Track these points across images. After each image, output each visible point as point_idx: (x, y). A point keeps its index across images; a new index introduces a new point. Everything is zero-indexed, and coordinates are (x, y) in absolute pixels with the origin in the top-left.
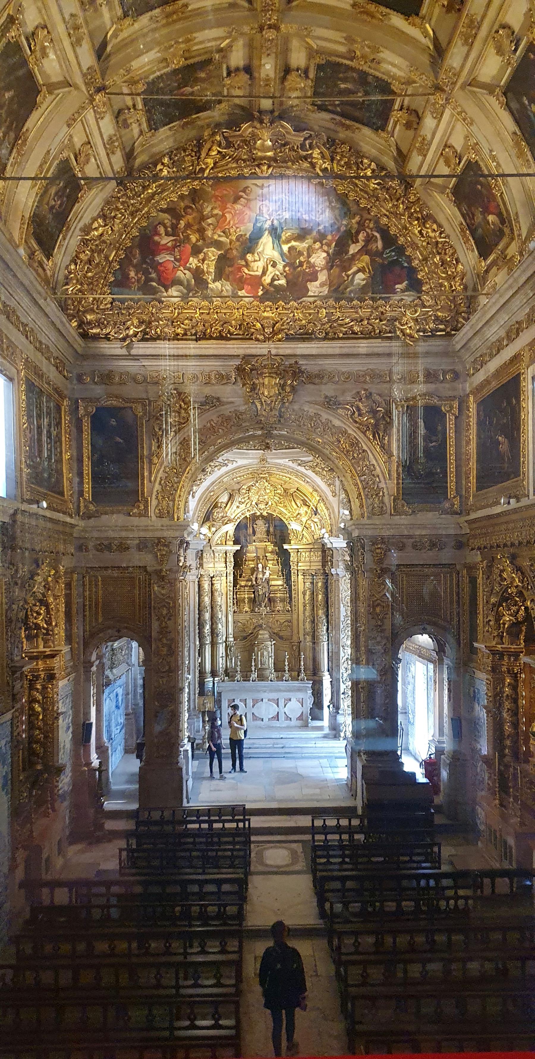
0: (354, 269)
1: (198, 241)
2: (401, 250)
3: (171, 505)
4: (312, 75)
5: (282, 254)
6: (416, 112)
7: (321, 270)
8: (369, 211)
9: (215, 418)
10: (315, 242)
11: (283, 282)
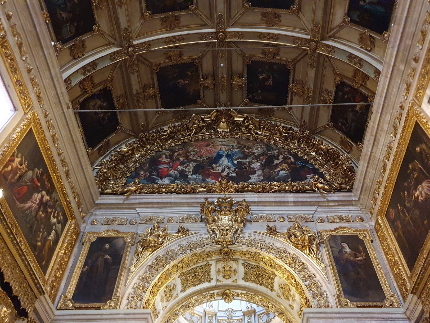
1: (184, 160)
2: (307, 162)
3: (139, 305)
4: (245, 75)
5: (233, 164)
7: (258, 170)
9: (184, 243)
10: (253, 159)
11: (234, 175)
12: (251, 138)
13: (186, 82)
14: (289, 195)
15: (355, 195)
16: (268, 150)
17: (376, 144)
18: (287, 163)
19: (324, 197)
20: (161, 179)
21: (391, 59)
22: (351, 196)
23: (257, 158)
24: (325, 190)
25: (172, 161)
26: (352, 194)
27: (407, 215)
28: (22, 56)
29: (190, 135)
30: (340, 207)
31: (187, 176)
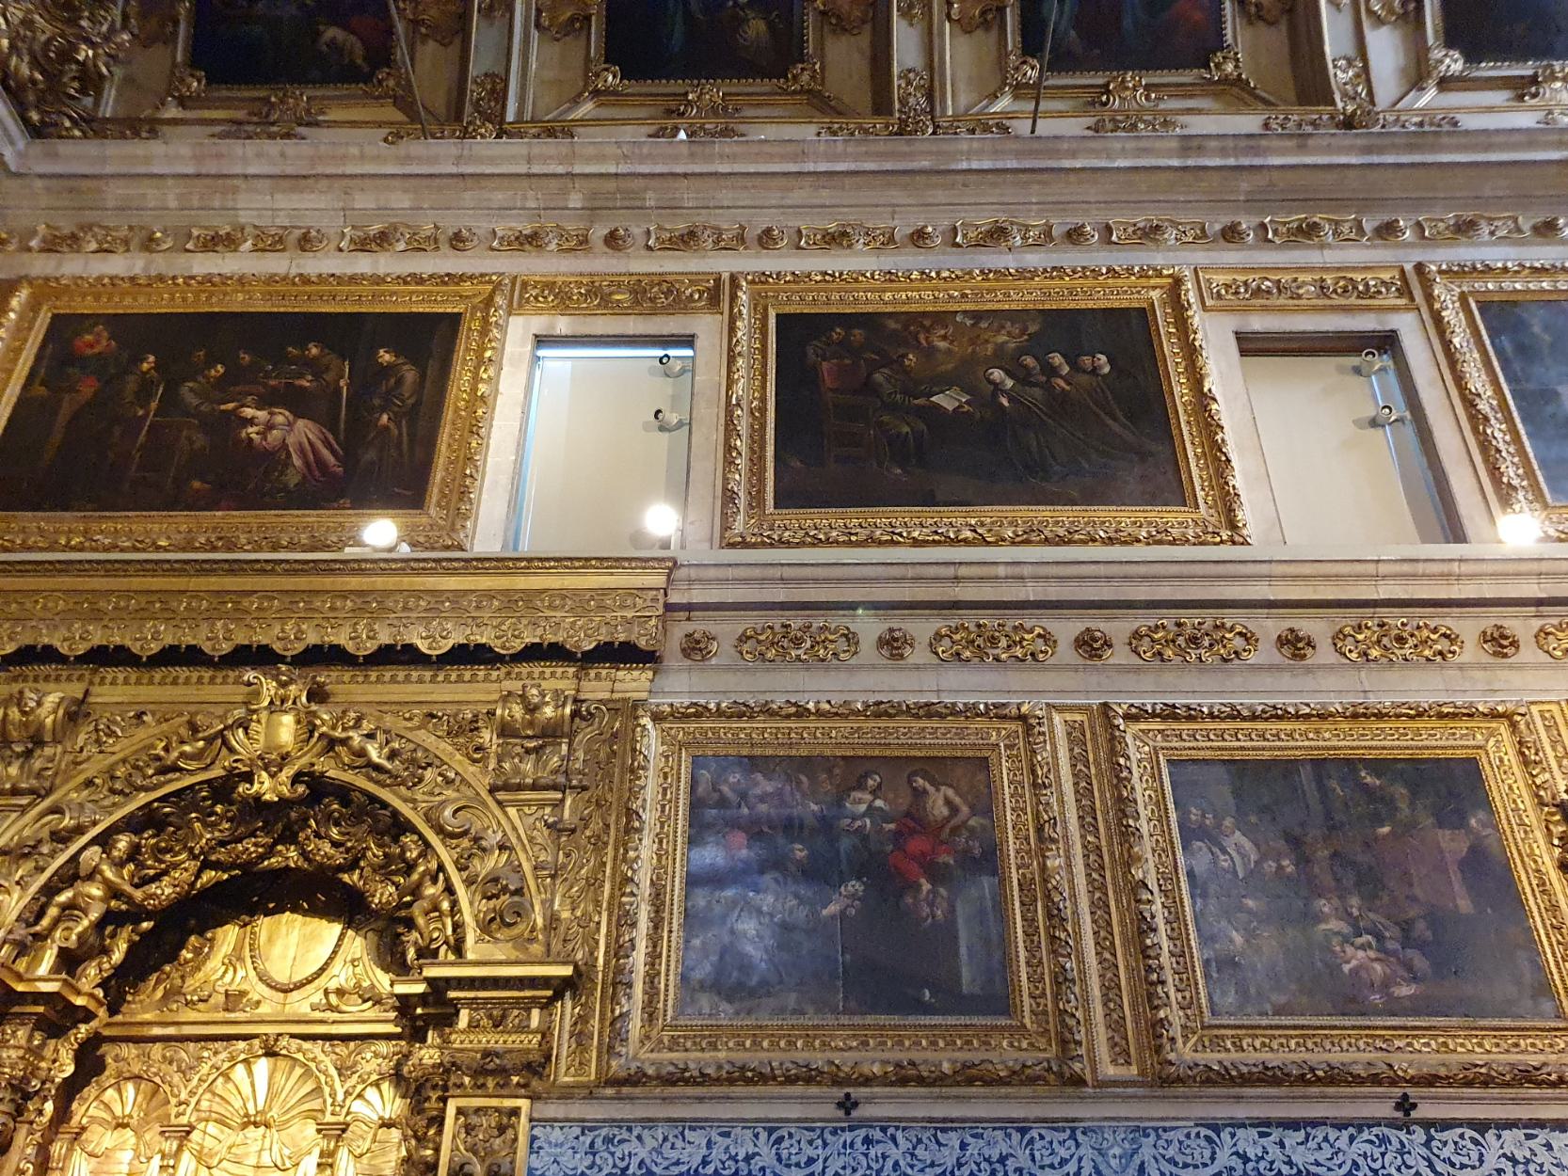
15: (20, 155)
17: (286, 184)
21: (589, 160)
22: (12, 143)
26: (21, 144)
27: (154, 405)
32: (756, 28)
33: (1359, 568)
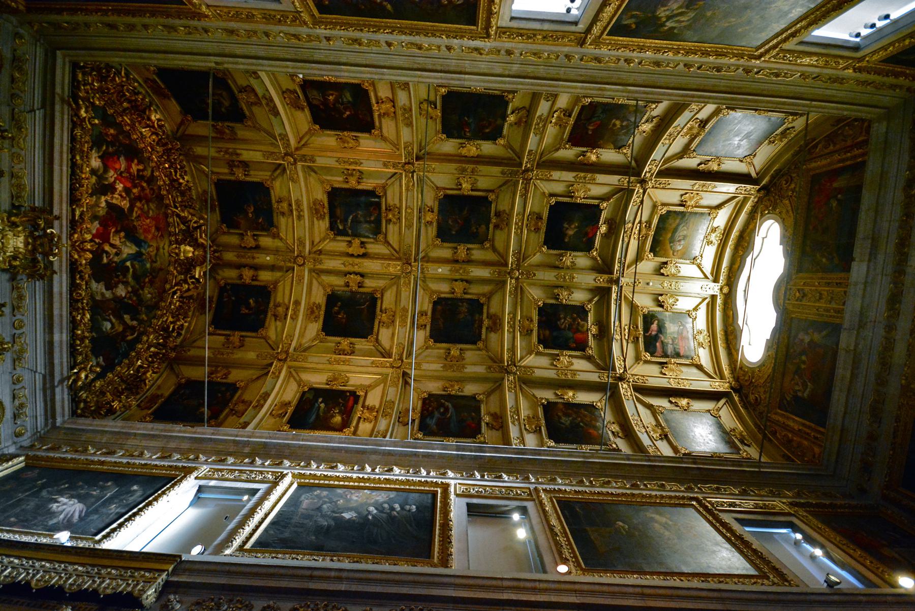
0: (114, 320)
2: (126, 355)
6: (242, 346)
7: (113, 294)
8: (150, 326)
10: (132, 287)
11: (105, 260)
12: (168, 286)
13: (250, 215)
14: (64, 336)
15: (64, 422)
16: (147, 307)
18: (124, 330)
19: (61, 382)
20: (99, 157)
22: (63, 416)
23: (135, 292)
24: (75, 381)
25: (131, 178)
28: (285, 34)
29: (176, 208)
30: (42, 404)
31: (105, 195)
32: (338, 419)
33: (494, 583)
